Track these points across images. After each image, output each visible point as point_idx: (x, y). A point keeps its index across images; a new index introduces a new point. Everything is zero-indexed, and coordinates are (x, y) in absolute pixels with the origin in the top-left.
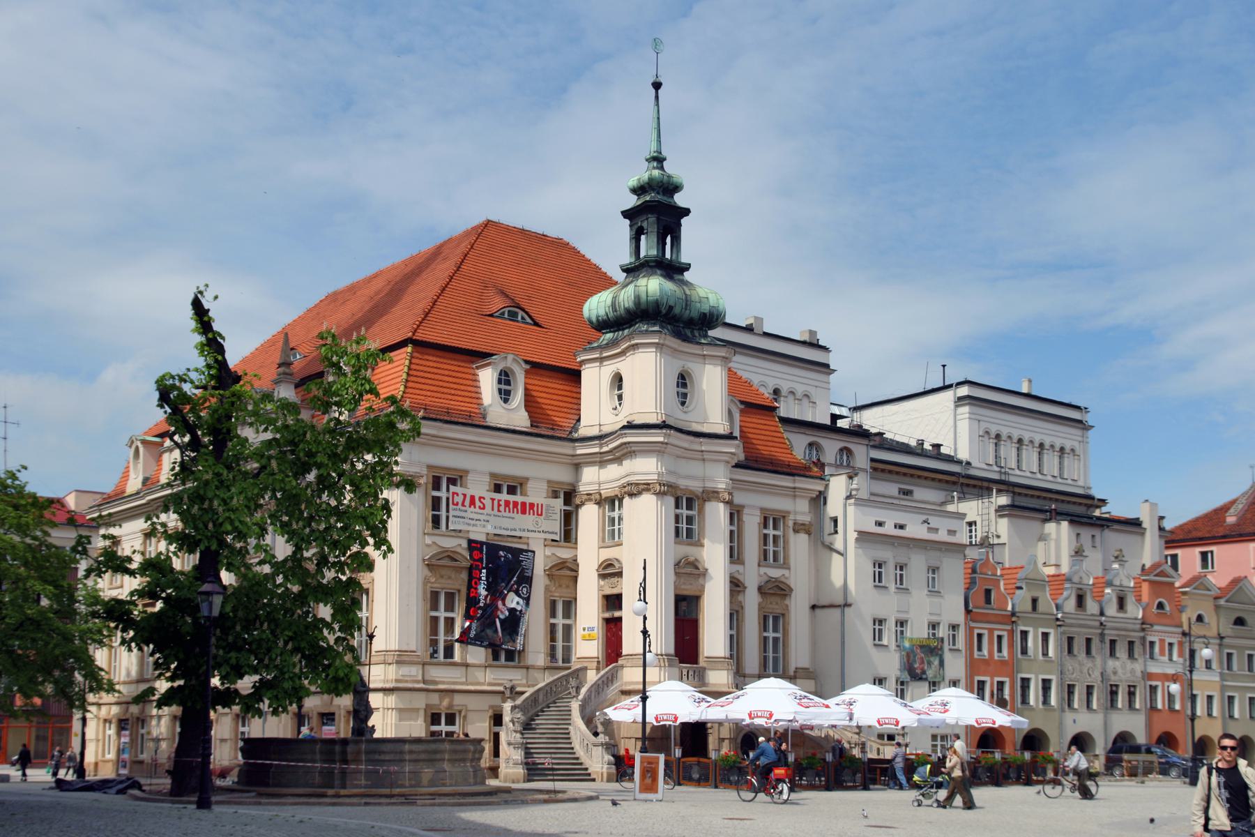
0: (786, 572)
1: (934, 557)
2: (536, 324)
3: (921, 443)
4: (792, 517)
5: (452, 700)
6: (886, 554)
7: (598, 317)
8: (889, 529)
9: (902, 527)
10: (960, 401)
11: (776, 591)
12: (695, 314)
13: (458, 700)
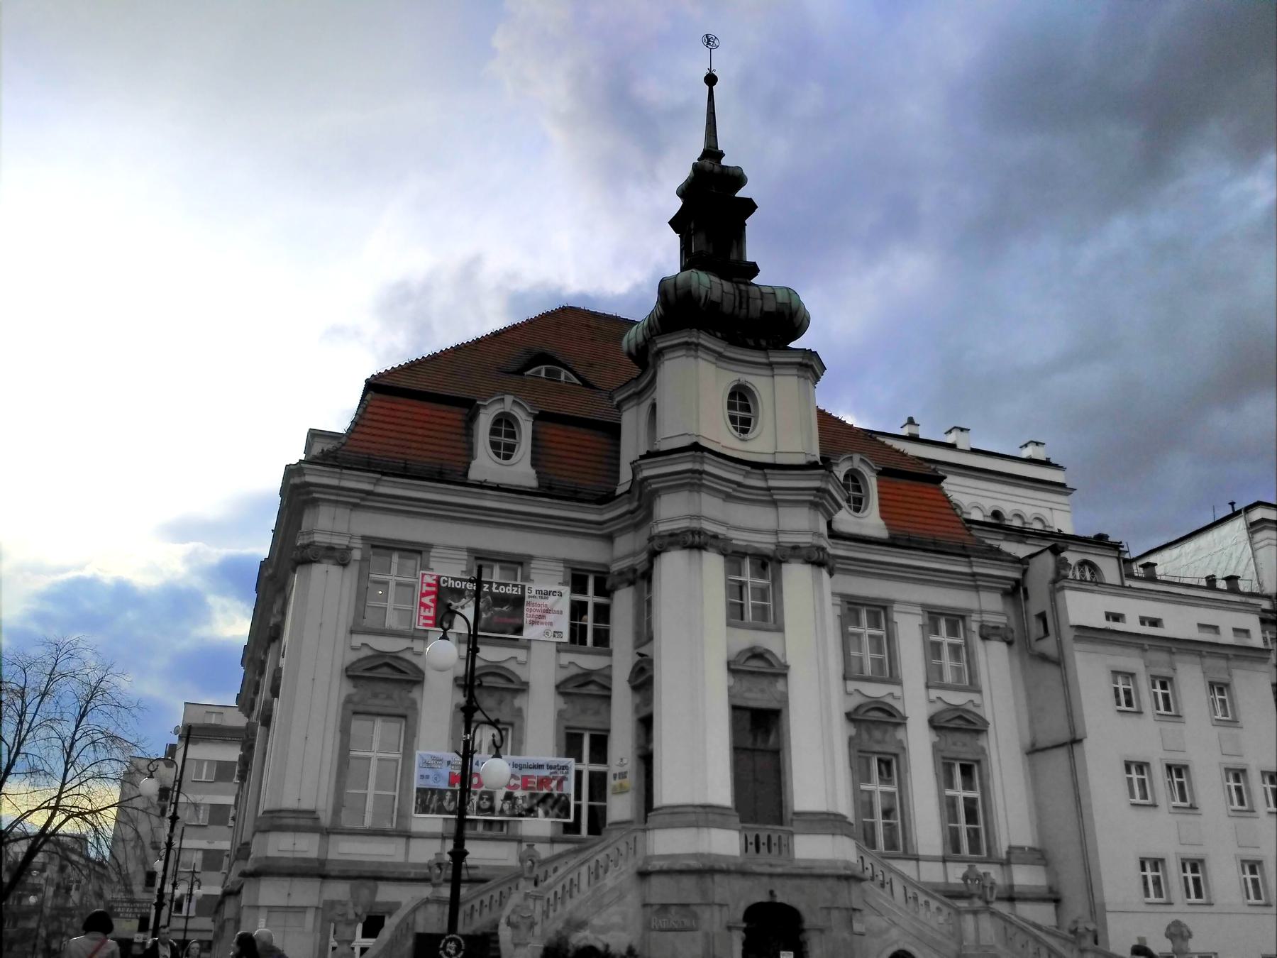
0: (974, 697)
1: (1219, 669)
2: (586, 384)
3: (1211, 580)
4: (975, 617)
5: (374, 892)
6: (1130, 661)
7: (637, 345)
8: (1131, 625)
9: (1155, 623)
10: (1254, 527)
11: (957, 726)
12: (754, 313)
13: (387, 893)
